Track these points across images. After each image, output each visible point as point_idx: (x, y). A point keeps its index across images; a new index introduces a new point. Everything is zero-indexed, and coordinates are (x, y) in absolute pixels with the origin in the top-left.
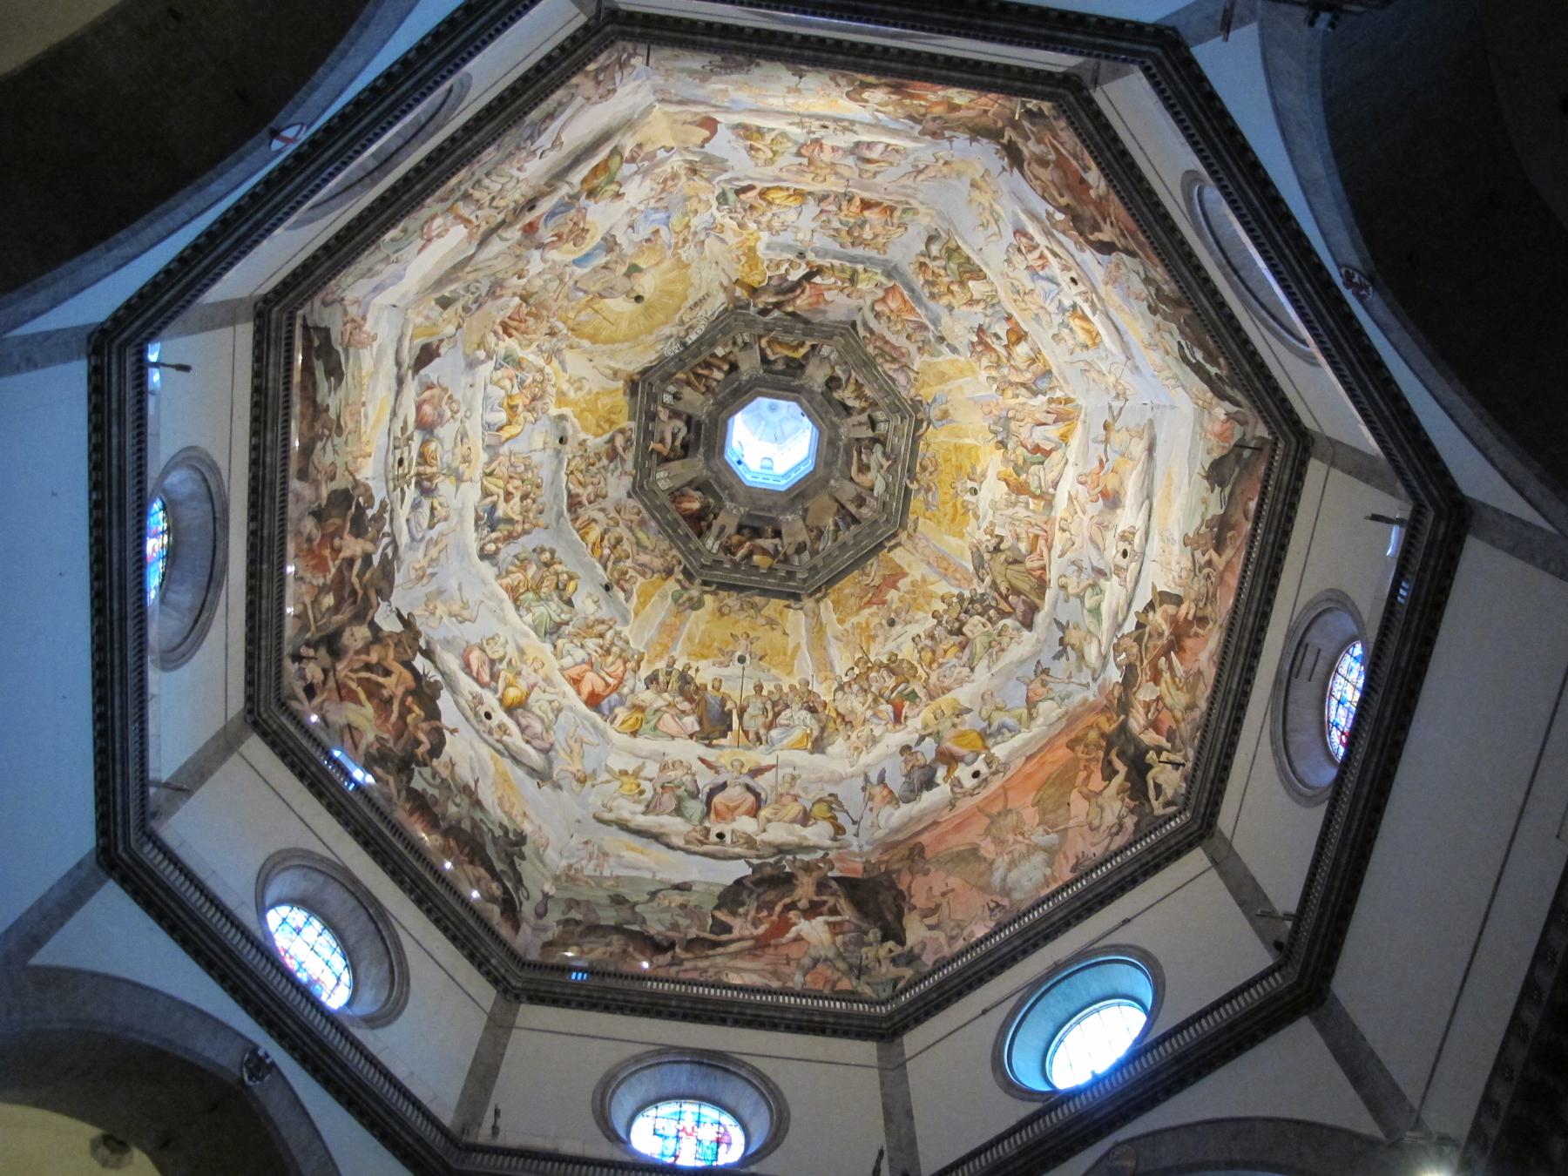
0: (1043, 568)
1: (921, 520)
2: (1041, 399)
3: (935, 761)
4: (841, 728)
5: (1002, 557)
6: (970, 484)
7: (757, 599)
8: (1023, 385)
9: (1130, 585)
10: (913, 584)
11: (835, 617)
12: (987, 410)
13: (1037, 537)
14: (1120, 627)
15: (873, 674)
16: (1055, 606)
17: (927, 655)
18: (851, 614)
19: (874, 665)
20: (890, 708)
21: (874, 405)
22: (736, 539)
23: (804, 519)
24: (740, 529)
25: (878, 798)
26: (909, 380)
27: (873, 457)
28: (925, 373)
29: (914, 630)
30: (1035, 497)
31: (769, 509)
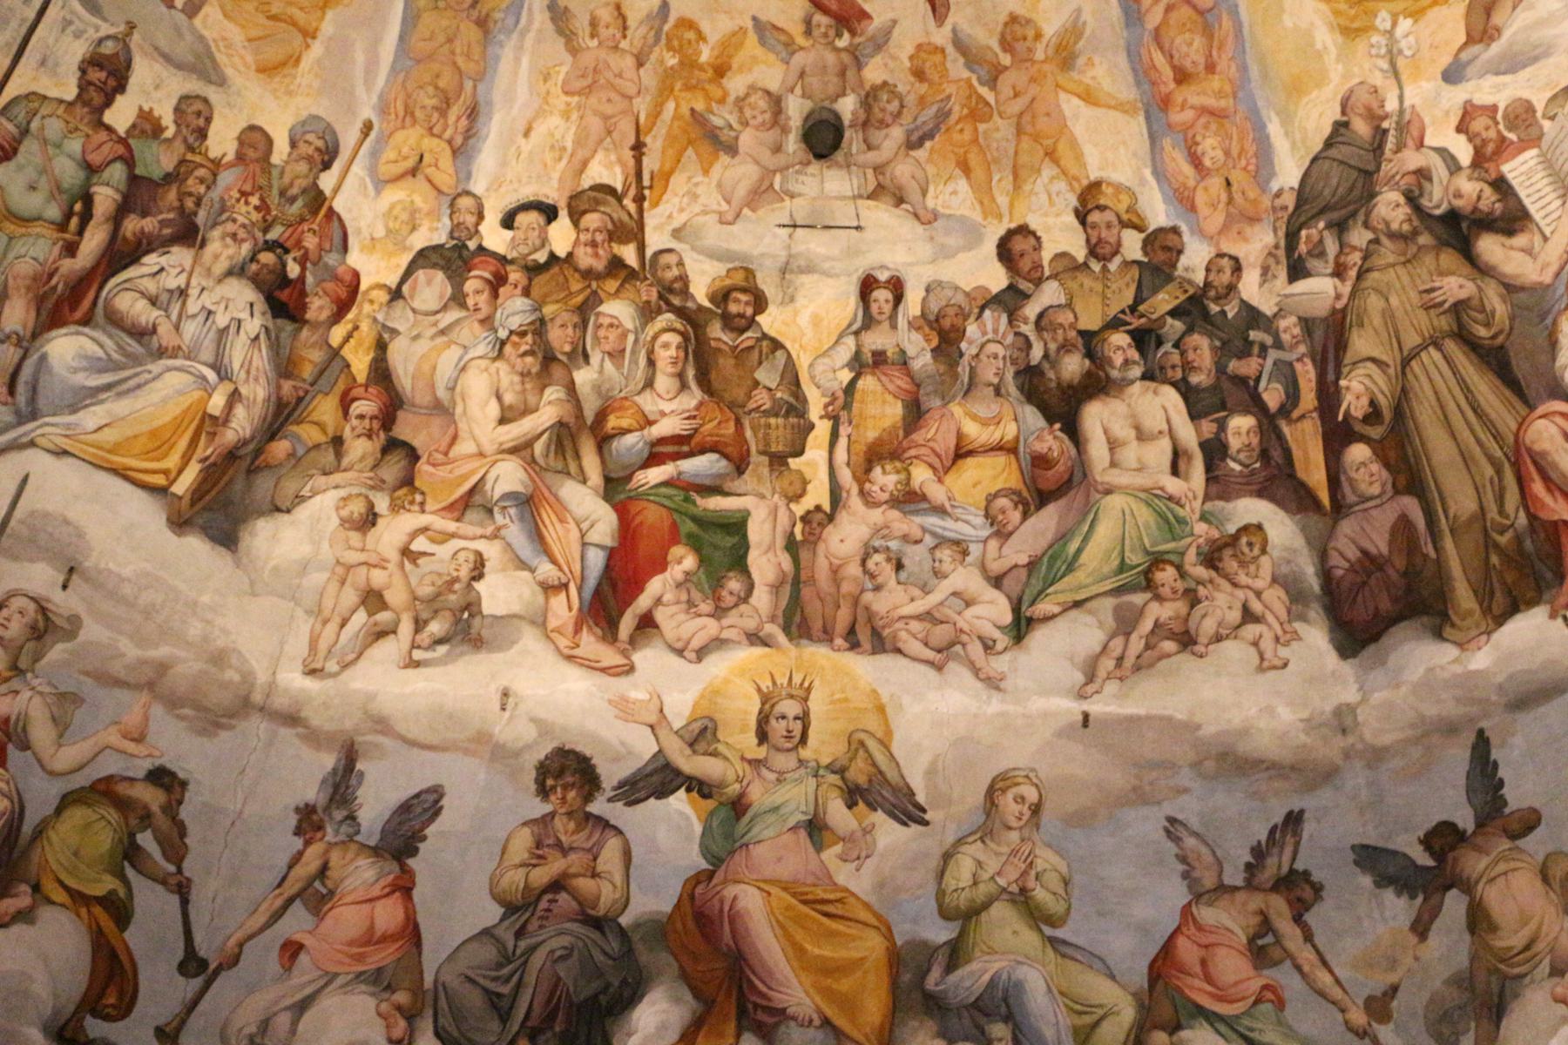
3: (660, 930)
4: (359, 448)
5: (1456, 286)
15: (618, 309)
19: (651, 264)
20: (603, 523)
25: (346, 920)
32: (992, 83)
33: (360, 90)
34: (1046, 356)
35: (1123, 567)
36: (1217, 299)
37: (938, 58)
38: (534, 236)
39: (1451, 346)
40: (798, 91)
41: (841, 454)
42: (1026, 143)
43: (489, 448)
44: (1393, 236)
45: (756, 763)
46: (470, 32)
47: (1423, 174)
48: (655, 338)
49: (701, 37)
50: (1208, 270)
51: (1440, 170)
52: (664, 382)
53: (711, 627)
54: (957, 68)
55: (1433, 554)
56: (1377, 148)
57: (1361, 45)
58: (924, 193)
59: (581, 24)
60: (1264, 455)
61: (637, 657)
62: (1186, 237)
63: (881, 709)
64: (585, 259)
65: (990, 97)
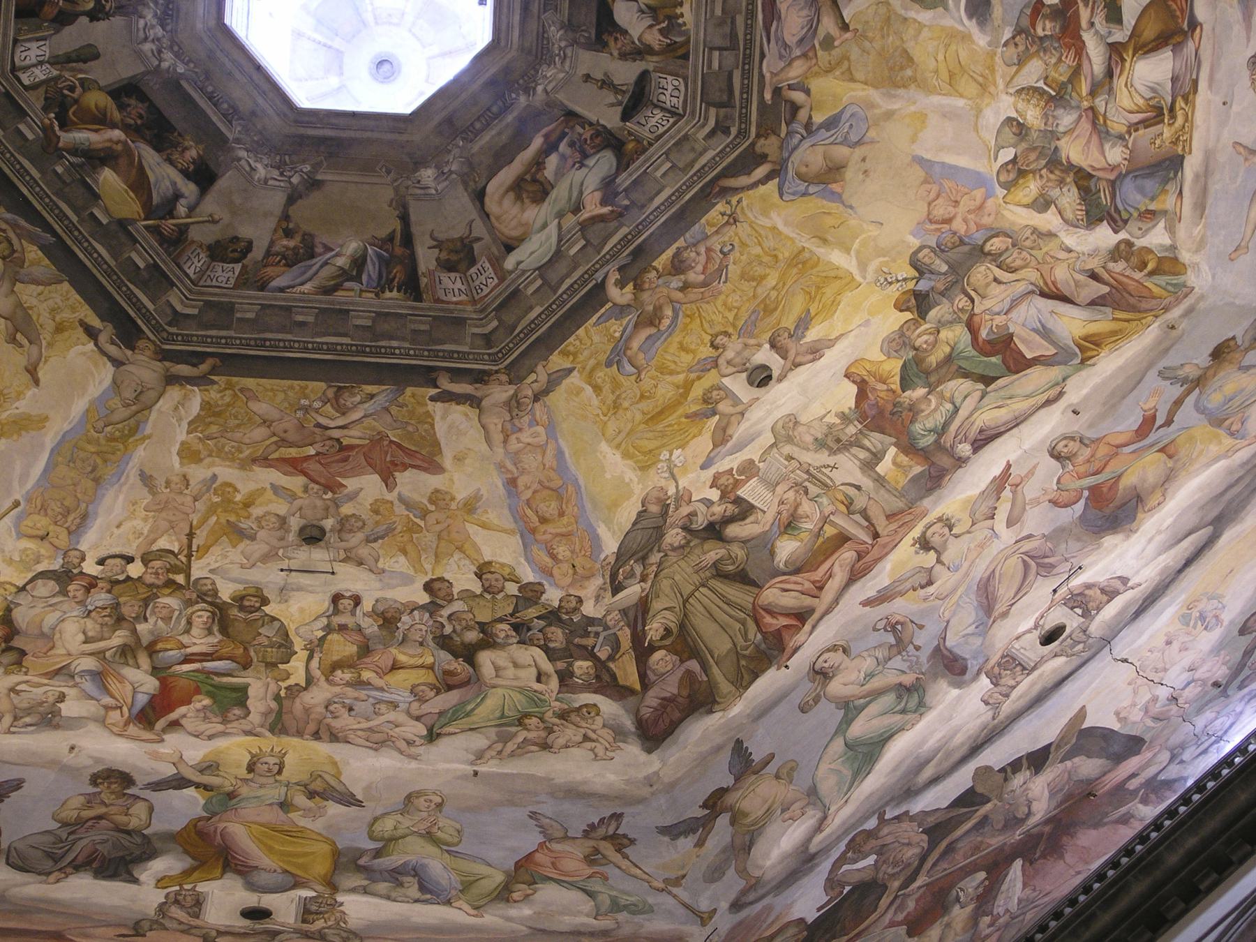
0: (801, 616)
1: (575, 379)
2: (1104, 237)
5: (713, 553)
6: (765, 356)
7: (33, 253)
8: (1083, 179)
9: (1007, 707)
10: (437, 497)
11: (181, 435)
12: (940, 211)
13: (843, 539)
14: (910, 792)
15: (170, 601)
16: (762, 712)
17: (342, 647)
18: (230, 458)
20: (150, 685)
21: (677, 53)
22: (96, 99)
23: (291, 200)
24: (125, 92)
26: (813, 27)
27: (578, 175)
28: (860, 36)
29: (351, 580)
30: (909, 447)
31: (231, 115)
32: (423, 518)
33: (16, 484)
34: (454, 631)
35: (502, 716)
36: (567, 613)
37: (389, 505)
38: (118, 569)
39: (712, 583)
40: (298, 515)
41: (315, 663)
42: (443, 544)
43: (73, 651)
44: (674, 549)
45: (245, 780)
46: (90, 484)
47: (693, 514)
48: (193, 613)
49: (236, 490)
50: (561, 601)
51: (702, 508)
52: (195, 631)
53: (220, 727)
54: (400, 510)
55: (705, 679)
56: (664, 513)
57: (652, 472)
58: (377, 561)
59: (160, 482)
60: (598, 677)
61: (166, 737)
62: (547, 586)
63: (335, 764)
64: (150, 579)
65: (422, 524)
